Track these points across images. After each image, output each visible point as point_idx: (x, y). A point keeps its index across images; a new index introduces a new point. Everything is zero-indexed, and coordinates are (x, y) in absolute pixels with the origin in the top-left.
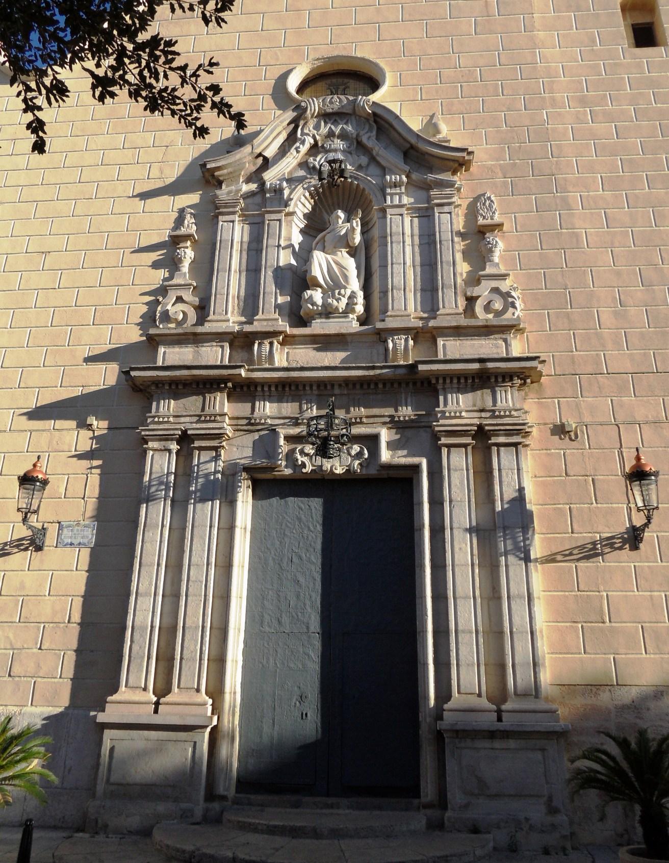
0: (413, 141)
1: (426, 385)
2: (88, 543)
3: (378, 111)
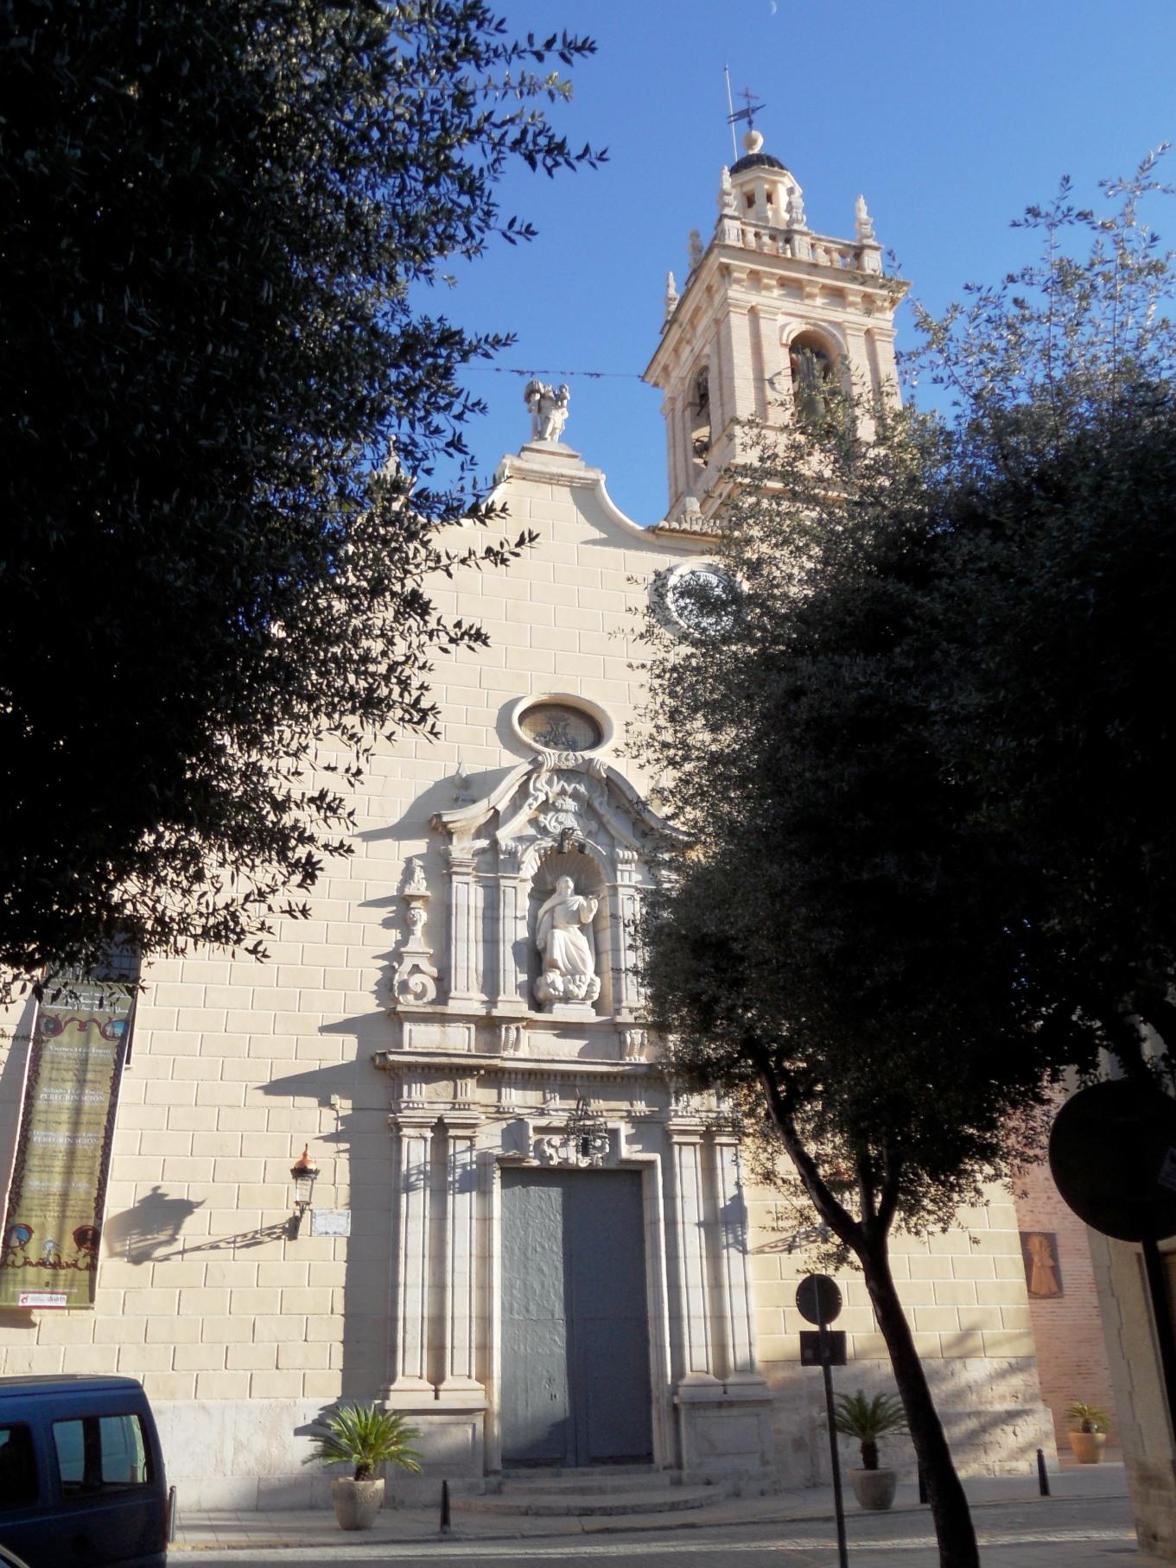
3: (612, 776)
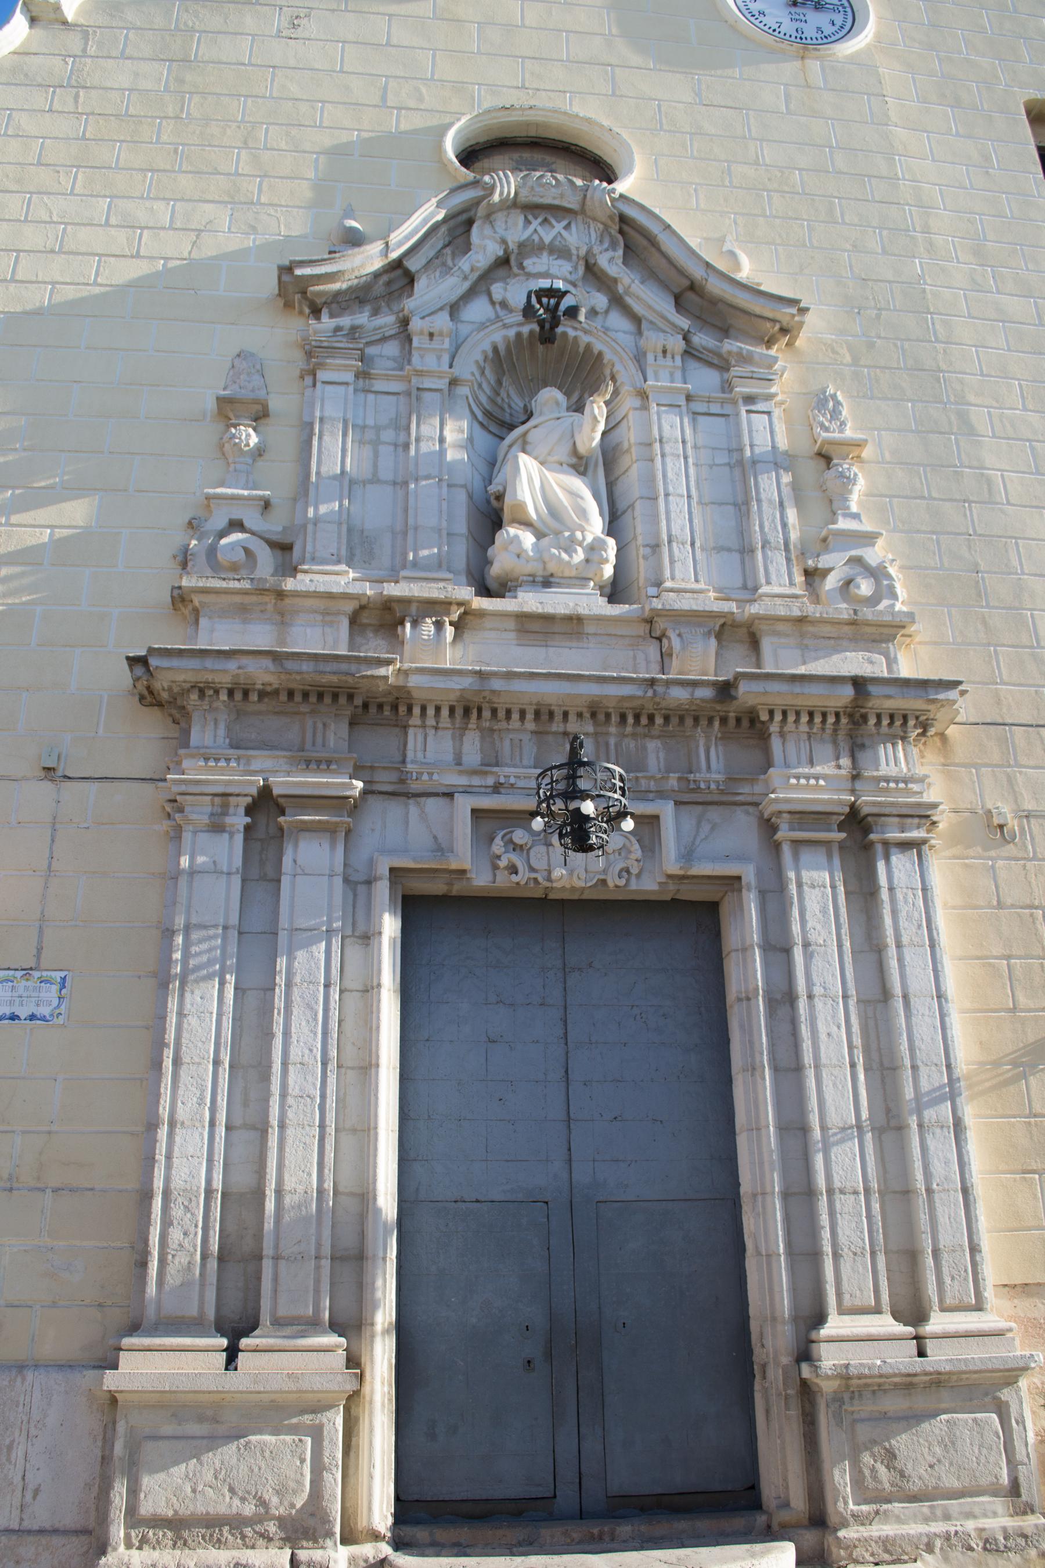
0: (698, 273)
1: (745, 723)
2: (52, 1015)
